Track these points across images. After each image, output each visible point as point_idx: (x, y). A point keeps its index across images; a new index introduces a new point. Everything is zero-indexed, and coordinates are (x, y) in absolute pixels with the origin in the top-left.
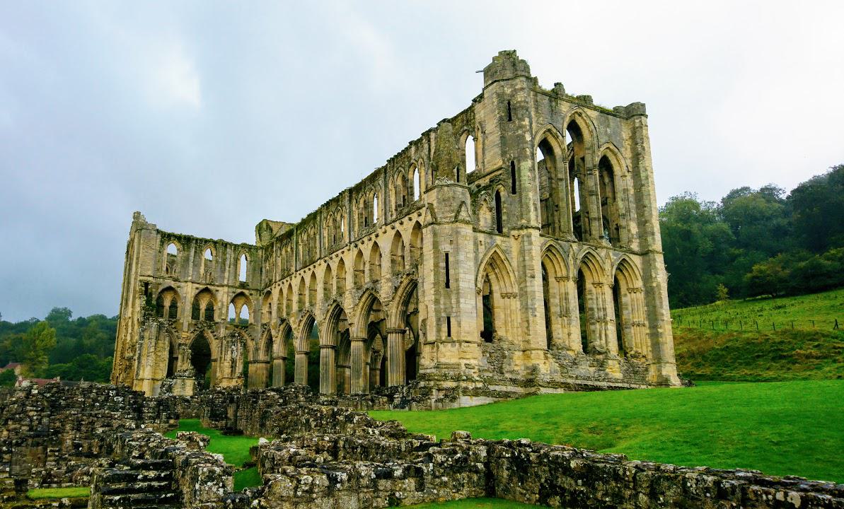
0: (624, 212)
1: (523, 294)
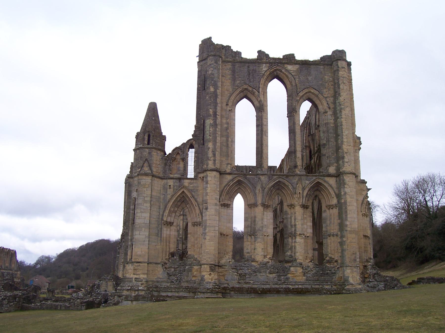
0: (325, 142)
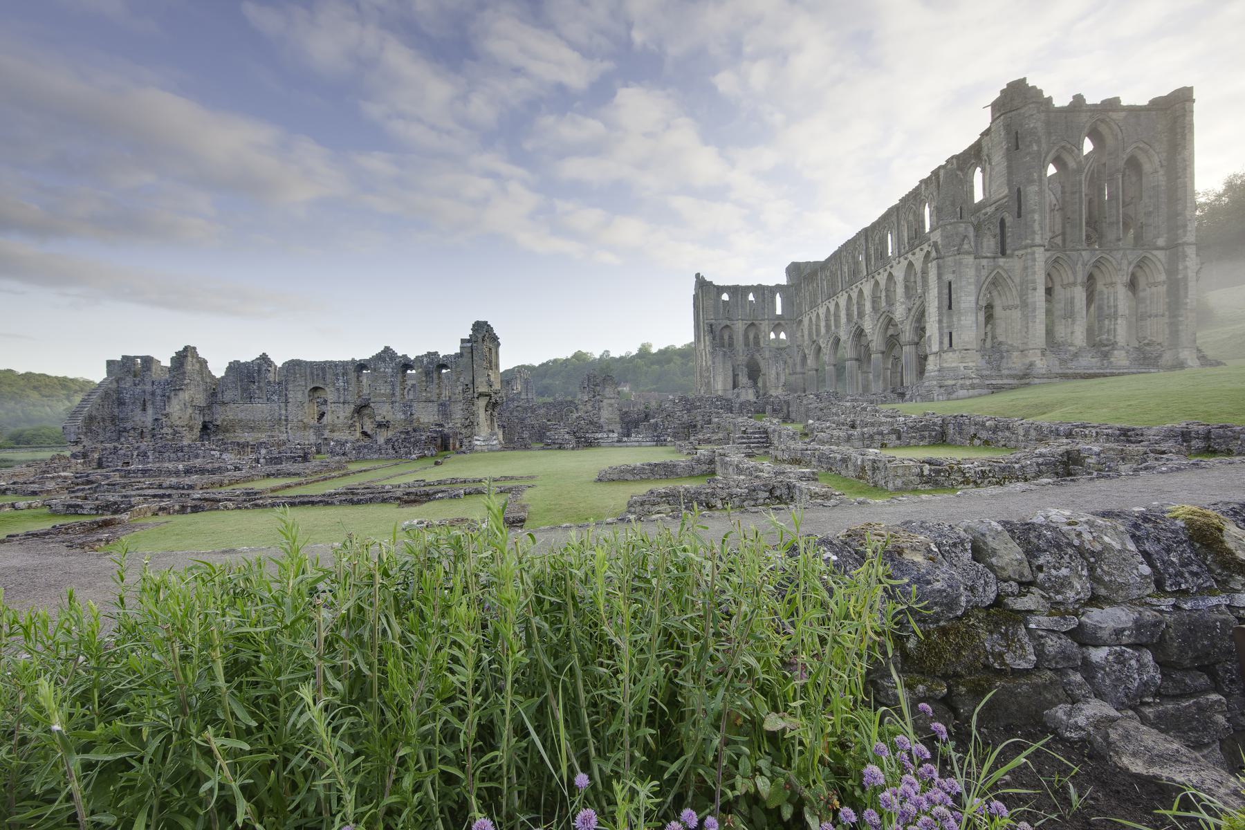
1: (1024, 304)
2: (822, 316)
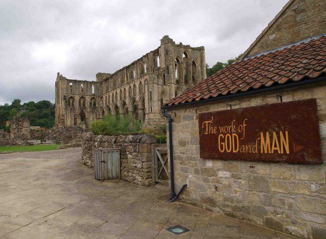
2: (111, 96)
